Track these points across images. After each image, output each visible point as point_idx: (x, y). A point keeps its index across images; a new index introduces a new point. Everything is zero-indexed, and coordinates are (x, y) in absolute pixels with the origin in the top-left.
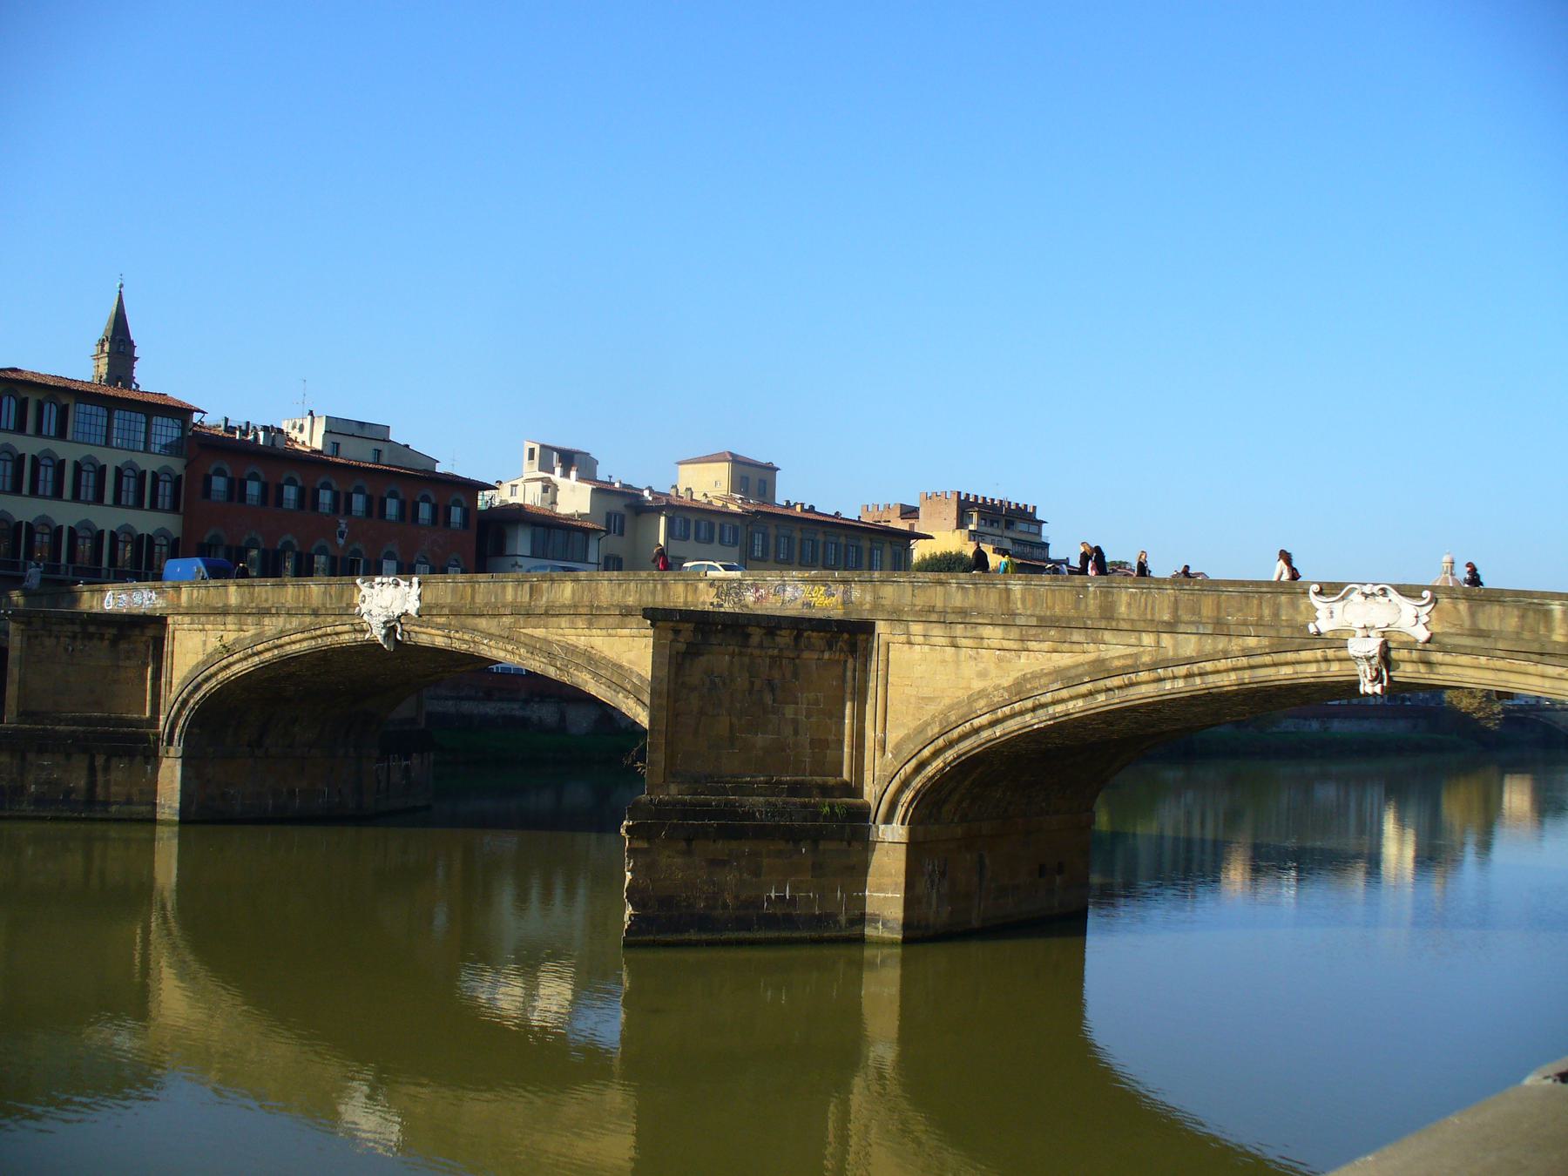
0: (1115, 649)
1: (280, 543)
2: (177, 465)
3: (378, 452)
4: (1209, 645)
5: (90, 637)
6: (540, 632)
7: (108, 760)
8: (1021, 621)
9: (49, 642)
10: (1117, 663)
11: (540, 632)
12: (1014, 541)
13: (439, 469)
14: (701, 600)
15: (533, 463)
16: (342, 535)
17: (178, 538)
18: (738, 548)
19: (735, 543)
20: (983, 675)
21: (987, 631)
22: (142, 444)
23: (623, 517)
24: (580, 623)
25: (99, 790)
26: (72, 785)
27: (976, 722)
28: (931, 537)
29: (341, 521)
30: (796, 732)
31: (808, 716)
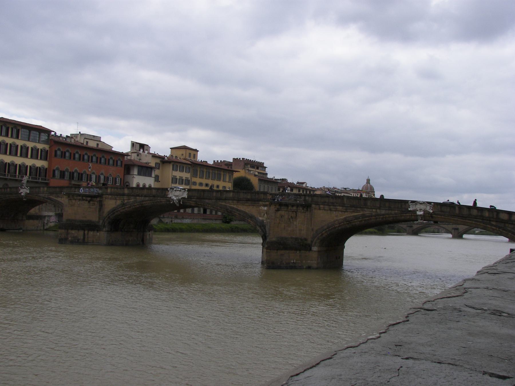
0: (367, 212)
1: (74, 170)
2: (47, 147)
3: (98, 144)
4: (387, 212)
5: (84, 200)
6: (223, 204)
7: (88, 232)
8: (346, 205)
9: (74, 201)
10: (367, 215)
11: (223, 204)
12: (258, 172)
13: (113, 149)
14: (268, 198)
15: (133, 148)
16: (90, 168)
17: (47, 168)
18: (190, 174)
19: (189, 172)
20: (337, 216)
21: (338, 207)
22: (38, 141)
23: (159, 164)
24: (235, 202)
25: (86, 239)
26: (79, 238)
27: (336, 226)
28: (239, 172)
29: (90, 164)
30: (296, 227)
31: (298, 224)
